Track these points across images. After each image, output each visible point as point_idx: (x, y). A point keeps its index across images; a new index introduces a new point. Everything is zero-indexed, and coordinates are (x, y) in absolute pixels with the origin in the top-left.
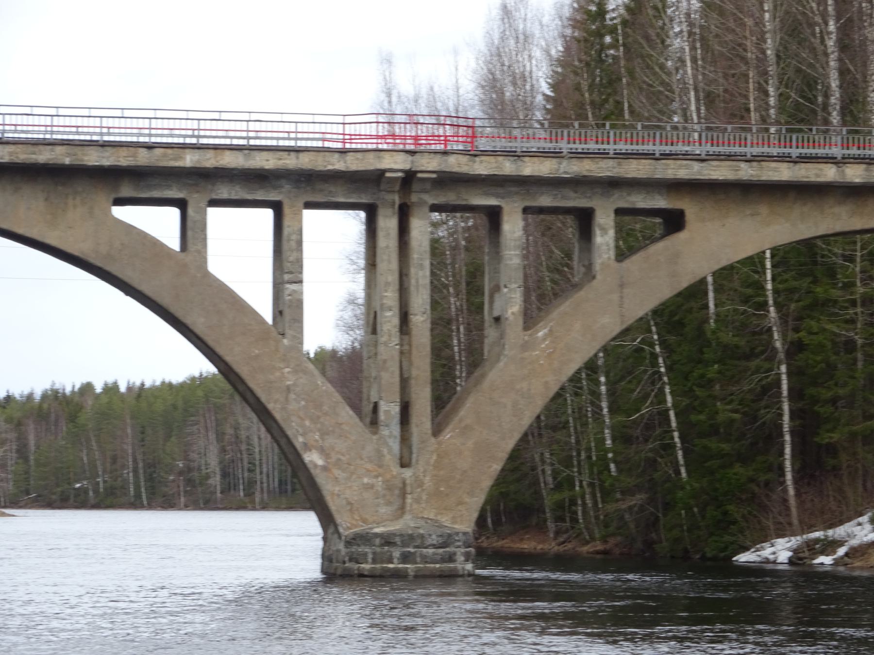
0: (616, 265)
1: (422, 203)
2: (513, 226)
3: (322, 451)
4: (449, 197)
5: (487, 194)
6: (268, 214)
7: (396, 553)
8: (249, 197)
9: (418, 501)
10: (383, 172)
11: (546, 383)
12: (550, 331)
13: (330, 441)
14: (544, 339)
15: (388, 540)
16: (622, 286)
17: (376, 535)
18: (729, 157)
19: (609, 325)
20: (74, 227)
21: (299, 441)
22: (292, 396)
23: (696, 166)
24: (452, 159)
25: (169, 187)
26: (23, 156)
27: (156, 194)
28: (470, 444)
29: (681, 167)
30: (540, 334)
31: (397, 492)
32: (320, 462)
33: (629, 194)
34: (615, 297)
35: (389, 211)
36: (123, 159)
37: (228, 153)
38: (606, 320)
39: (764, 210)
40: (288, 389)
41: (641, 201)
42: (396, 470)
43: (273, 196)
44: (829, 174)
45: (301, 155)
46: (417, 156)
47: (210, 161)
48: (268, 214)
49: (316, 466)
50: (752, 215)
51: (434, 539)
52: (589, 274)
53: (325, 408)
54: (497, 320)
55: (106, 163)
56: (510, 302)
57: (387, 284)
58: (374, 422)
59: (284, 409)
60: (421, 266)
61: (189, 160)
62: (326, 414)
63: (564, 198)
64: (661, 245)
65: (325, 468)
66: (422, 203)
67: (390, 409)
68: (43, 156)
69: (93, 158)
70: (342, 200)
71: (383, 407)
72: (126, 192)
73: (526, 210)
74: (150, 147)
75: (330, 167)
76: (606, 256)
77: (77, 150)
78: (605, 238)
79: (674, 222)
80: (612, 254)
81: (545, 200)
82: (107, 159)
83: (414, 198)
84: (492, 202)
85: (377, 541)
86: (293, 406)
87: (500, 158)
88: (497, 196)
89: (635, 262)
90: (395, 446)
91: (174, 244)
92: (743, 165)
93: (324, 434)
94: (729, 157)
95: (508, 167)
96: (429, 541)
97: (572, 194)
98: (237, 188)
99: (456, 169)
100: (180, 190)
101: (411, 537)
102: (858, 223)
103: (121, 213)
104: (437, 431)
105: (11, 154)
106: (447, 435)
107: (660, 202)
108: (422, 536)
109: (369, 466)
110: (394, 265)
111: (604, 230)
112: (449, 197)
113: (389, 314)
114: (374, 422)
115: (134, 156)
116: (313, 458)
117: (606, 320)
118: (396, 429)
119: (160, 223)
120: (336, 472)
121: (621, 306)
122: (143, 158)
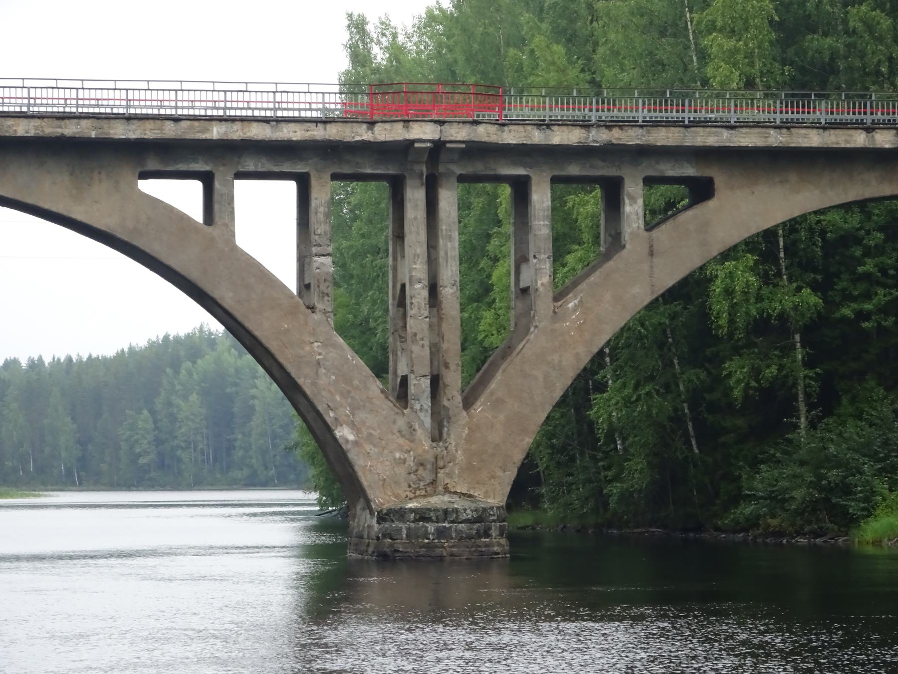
0: (646, 234)
1: (450, 173)
2: (541, 198)
3: (353, 426)
4: (478, 168)
5: (515, 164)
6: (291, 187)
8: (276, 169)
9: (449, 475)
10: (413, 141)
11: (577, 354)
12: (581, 301)
13: (361, 415)
15: (422, 516)
16: (651, 254)
17: (412, 510)
18: (758, 125)
19: (640, 295)
20: (100, 202)
21: (330, 416)
22: (322, 371)
23: (725, 133)
25: (195, 160)
26: (49, 129)
27: (182, 167)
28: (502, 417)
29: (710, 134)
30: (570, 305)
31: (429, 466)
32: (351, 437)
33: (657, 163)
34: (646, 267)
35: (417, 182)
36: (149, 132)
37: (255, 125)
38: (636, 290)
39: (793, 177)
40: (318, 363)
41: (670, 170)
42: (427, 444)
43: (300, 168)
44: (859, 139)
45: (328, 126)
46: (446, 126)
47: (236, 133)
48: (291, 187)
49: (347, 441)
50: (781, 182)
51: (469, 515)
52: (616, 243)
53: (356, 382)
54: (525, 291)
55: (132, 136)
56: (540, 274)
57: (416, 256)
59: (314, 384)
60: (450, 238)
61: (216, 132)
63: (592, 167)
64: (690, 213)
65: (356, 443)
66: (450, 173)
68: (70, 129)
69: (119, 131)
71: (412, 381)
72: (152, 165)
73: (555, 180)
74: (177, 119)
75: (358, 138)
76: (635, 225)
77: (104, 124)
78: (633, 209)
79: (701, 191)
81: (574, 170)
82: (133, 132)
83: (442, 169)
84: (521, 171)
86: (323, 381)
87: (529, 128)
88: (525, 166)
89: (663, 233)
90: (427, 420)
91: (197, 215)
92: (772, 132)
93: (354, 409)
94: (758, 125)
95: (537, 137)
96: (464, 517)
97: (600, 163)
98: (264, 160)
99: (485, 139)
100: (206, 163)
101: (446, 512)
102: (887, 190)
103: (148, 186)
104: (468, 403)
105: (36, 128)
106: (478, 408)
107: (689, 171)
108: (456, 511)
109: (401, 441)
110: (423, 236)
111: (633, 199)
112: (478, 168)
113: (418, 286)
115: (161, 129)
116: (344, 433)
117: (636, 290)
118: (427, 403)
119: (184, 196)
120: (368, 447)
121: (651, 276)
122: (170, 131)
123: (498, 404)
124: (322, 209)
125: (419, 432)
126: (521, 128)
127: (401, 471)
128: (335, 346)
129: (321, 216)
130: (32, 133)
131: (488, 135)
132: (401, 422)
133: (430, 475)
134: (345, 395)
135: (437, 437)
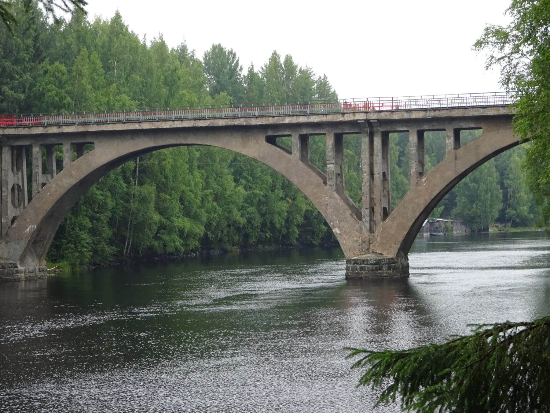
0: (454, 151)
1: (377, 131)
3: (339, 228)
5: (403, 126)
7: (358, 266)
8: (314, 132)
9: (374, 246)
12: (427, 178)
13: (342, 224)
14: (425, 182)
16: (456, 159)
17: (353, 260)
21: (331, 224)
22: (329, 207)
24: (382, 114)
25: (285, 131)
28: (395, 224)
29: (475, 111)
30: (423, 180)
31: (367, 243)
32: (339, 232)
33: (459, 123)
35: (365, 135)
37: (301, 117)
38: (449, 173)
40: (327, 204)
45: (328, 116)
46: (369, 114)
49: (337, 234)
51: (373, 262)
53: (341, 211)
55: (258, 123)
57: (365, 163)
58: (359, 217)
59: (326, 212)
60: (378, 156)
62: (341, 214)
65: (340, 234)
67: (366, 212)
70: (348, 131)
76: (450, 148)
77: (248, 120)
80: (452, 147)
83: (375, 129)
84: (405, 129)
85: (353, 262)
86: (329, 211)
87: (403, 112)
92: (501, 108)
93: (340, 221)
96: (370, 262)
97: (436, 124)
98: (310, 129)
101: (364, 261)
105: (225, 122)
108: (367, 260)
109: (357, 233)
110: (367, 155)
113: (365, 174)
114: (359, 217)
115: (268, 121)
116: (336, 231)
117: (449, 173)
120: (344, 236)
121: (455, 167)
123: (394, 218)
124: (330, 147)
125: (364, 230)
126: (400, 113)
127: (356, 245)
128: (334, 198)
129: (330, 149)
130: (224, 125)
131: (386, 116)
132: (357, 226)
133: (367, 245)
134: (337, 216)
135: (371, 231)
